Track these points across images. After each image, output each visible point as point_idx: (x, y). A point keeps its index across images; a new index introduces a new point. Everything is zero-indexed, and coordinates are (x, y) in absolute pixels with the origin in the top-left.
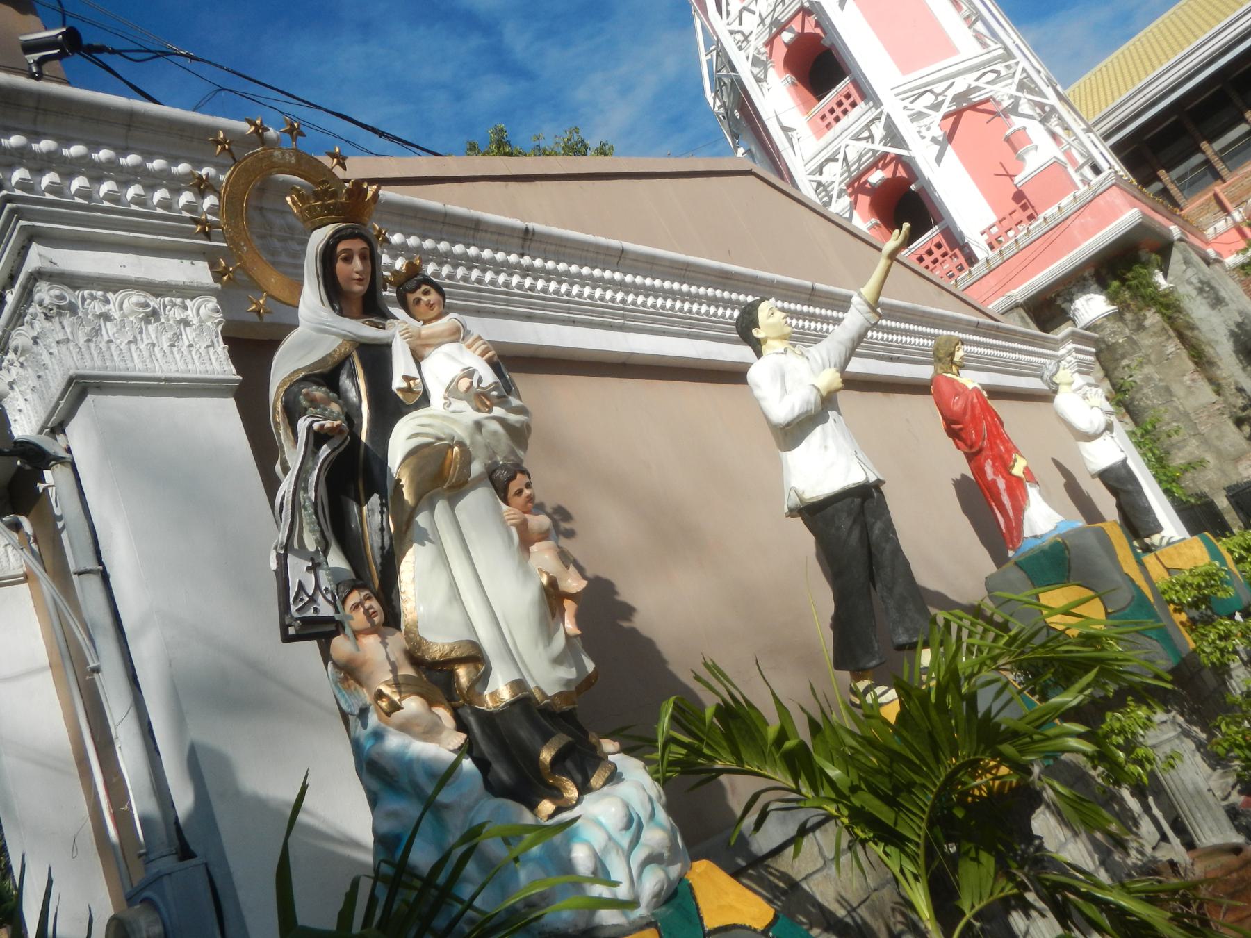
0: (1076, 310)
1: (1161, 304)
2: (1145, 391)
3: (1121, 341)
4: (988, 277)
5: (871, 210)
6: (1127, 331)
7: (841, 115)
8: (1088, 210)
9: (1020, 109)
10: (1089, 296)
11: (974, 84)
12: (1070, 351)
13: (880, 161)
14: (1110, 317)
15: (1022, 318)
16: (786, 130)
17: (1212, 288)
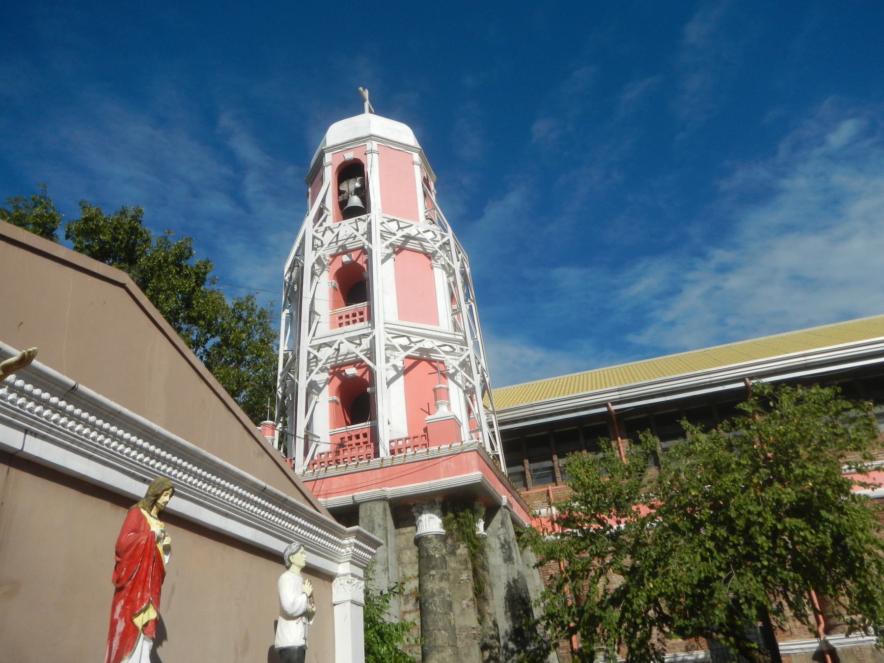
1: (472, 542)
2: (436, 599)
3: (437, 556)
4: (378, 471)
5: (337, 390)
6: (444, 551)
7: (351, 322)
11: (436, 348)
13: (357, 363)
14: (438, 536)
15: (385, 509)
16: (312, 312)
17: (510, 548)
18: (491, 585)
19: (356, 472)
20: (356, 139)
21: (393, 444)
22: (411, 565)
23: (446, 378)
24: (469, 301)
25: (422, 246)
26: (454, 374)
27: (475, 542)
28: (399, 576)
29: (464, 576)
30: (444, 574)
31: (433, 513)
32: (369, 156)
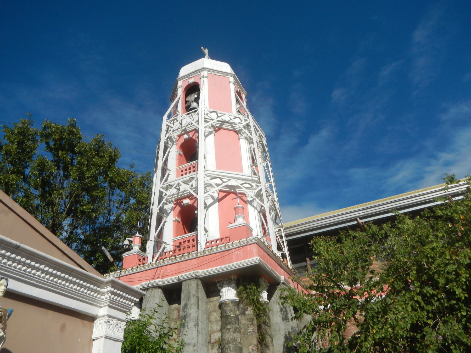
0: (222, 292)
1: (256, 306)
2: (230, 345)
3: (232, 316)
6: (238, 312)
9: (253, 203)
12: (108, 291)
13: (190, 196)
15: (198, 285)
17: (286, 311)
18: (271, 337)
20: (195, 71)
21: (208, 244)
22: (216, 322)
24: (266, 161)
25: (232, 126)
27: (258, 305)
28: (208, 330)
29: (250, 330)
30: (237, 328)
31: (230, 287)
32: (202, 79)
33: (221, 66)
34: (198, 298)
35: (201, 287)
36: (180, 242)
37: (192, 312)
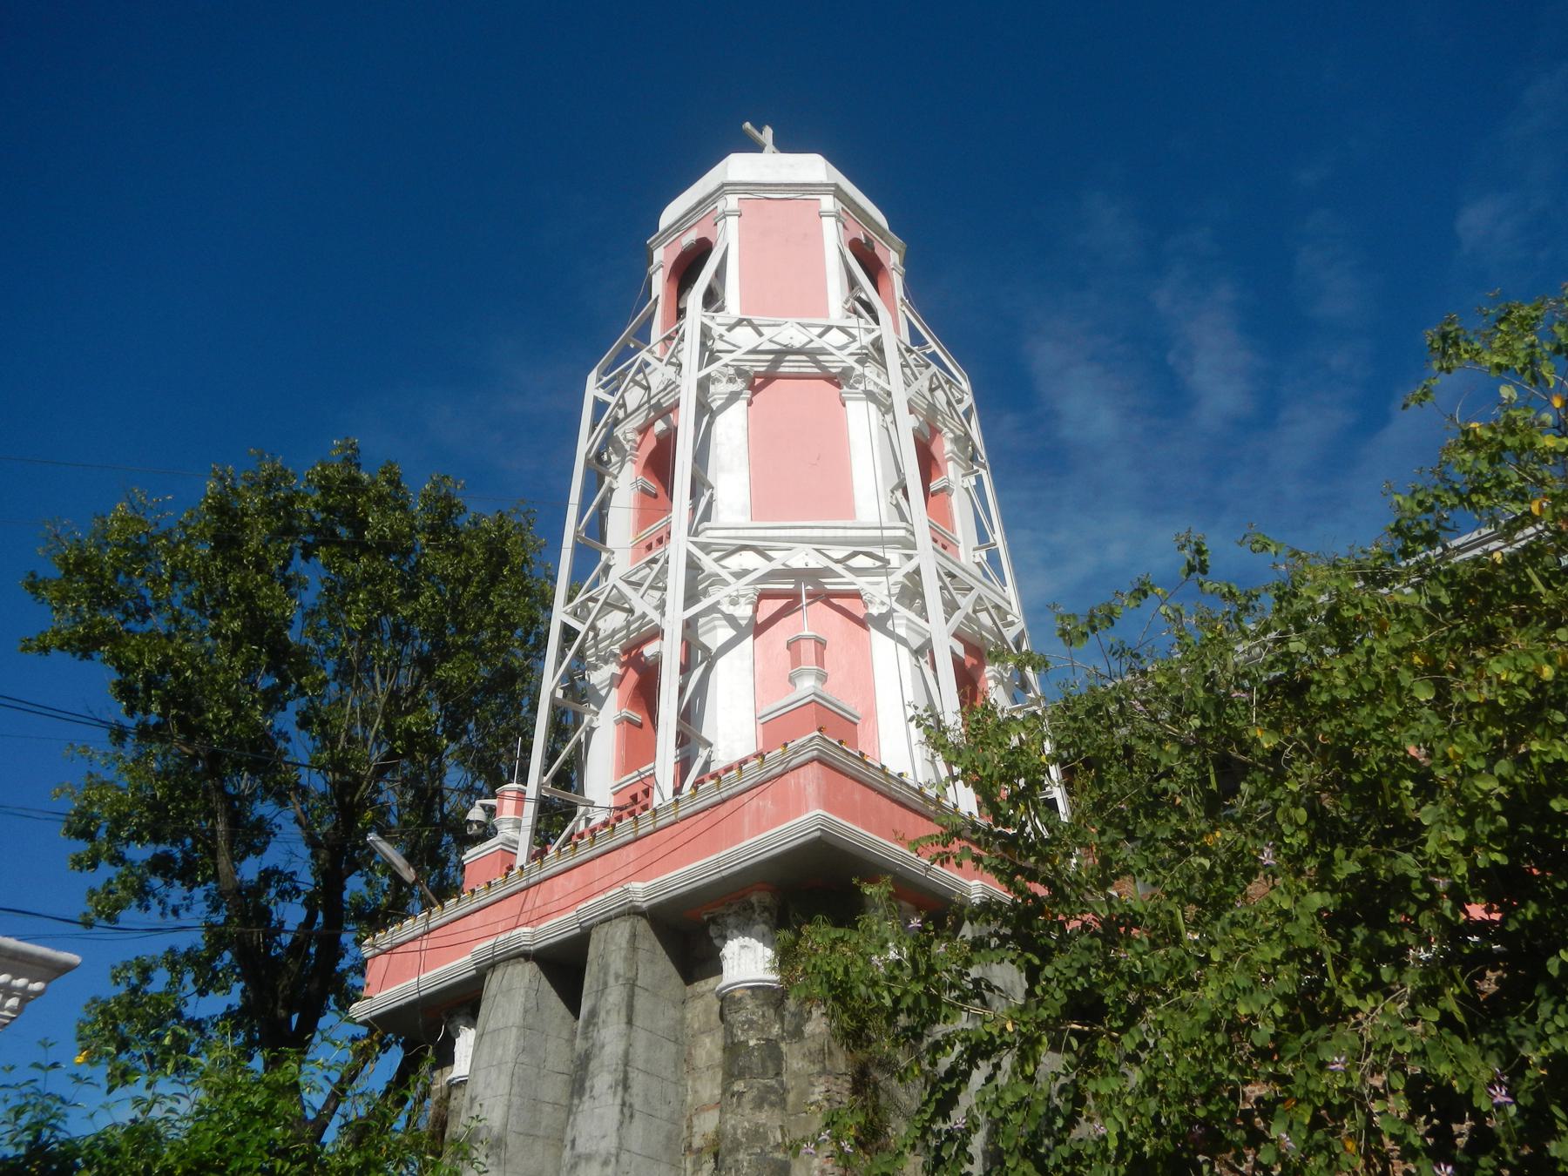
2: (741, 1156)
3: (752, 1043)
6: (776, 1029)
8: (773, 788)
10: (747, 941)
14: (760, 992)
15: (634, 936)
19: (592, 859)
20: (700, 203)
23: (868, 630)
25: (818, 363)
26: (889, 615)
30: (770, 1089)
31: (750, 936)
32: (720, 224)
33: (792, 166)
34: (632, 985)
35: (650, 942)
36: (632, 793)
37: (610, 1037)
